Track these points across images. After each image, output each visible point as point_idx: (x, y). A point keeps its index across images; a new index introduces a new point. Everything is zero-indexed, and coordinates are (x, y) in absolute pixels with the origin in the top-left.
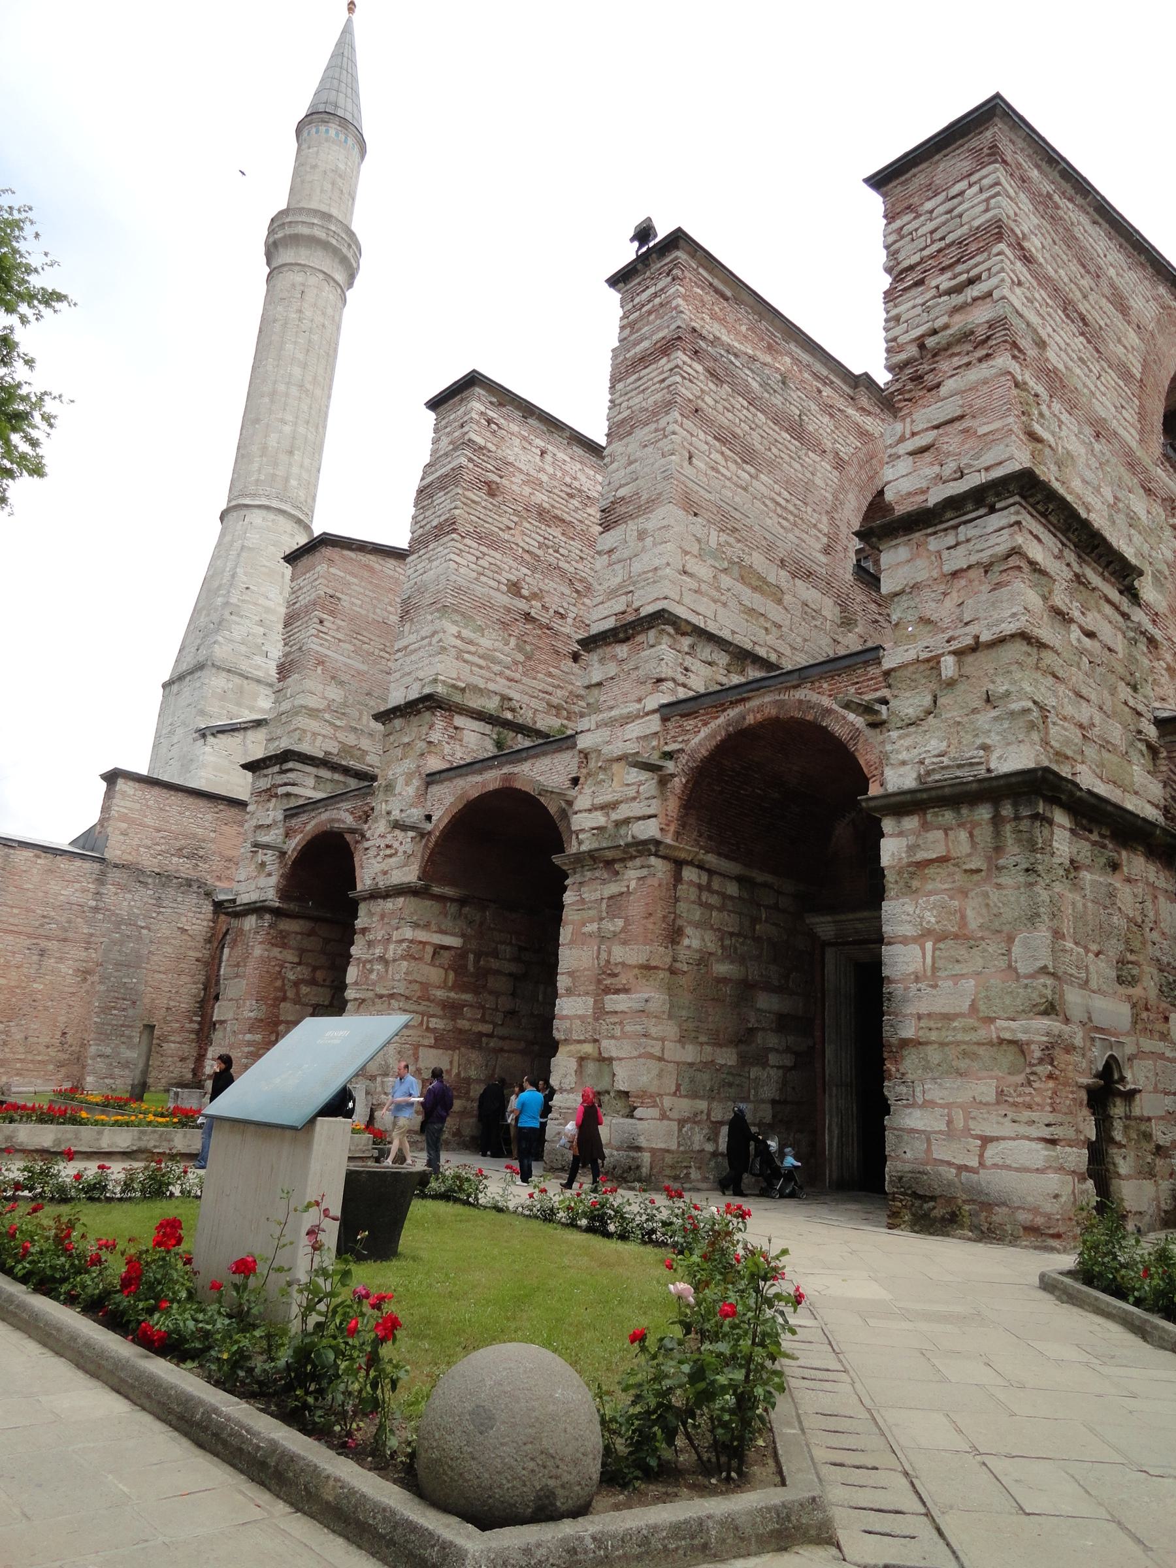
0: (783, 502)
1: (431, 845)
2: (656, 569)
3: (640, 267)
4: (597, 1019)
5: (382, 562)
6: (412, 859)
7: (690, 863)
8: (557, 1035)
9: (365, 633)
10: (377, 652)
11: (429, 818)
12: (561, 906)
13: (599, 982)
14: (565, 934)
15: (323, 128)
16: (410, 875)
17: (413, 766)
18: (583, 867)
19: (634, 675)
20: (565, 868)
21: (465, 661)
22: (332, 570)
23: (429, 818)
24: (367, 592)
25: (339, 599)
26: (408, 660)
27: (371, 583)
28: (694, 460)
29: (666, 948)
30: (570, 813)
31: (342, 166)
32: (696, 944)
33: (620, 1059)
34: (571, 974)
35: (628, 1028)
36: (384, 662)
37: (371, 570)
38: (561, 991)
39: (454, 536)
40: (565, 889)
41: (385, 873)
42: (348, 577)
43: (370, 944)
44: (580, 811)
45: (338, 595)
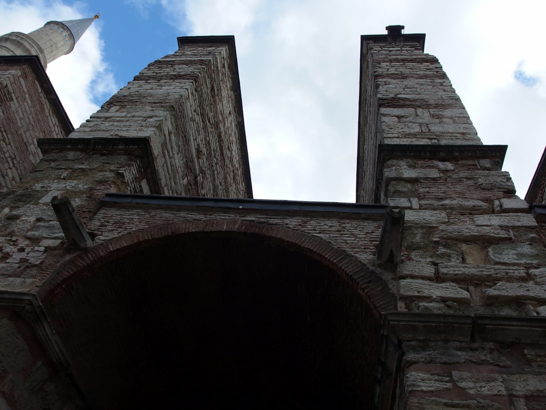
1: (82, 263)
2: (463, 134)
3: (390, 39)
5: (51, 113)
6: (34, 271)
9: (9, 136)
10: (7, 155)
15: (61, 30)
18: (446, 341)
19: (471, 182)
21: (163, 153)
22: (22, 80)
24: (30, 117)
25: (12, 99)
26: (107, 124)
27: (37, 114)
30: (387, 276)
31: (59, 45)
36: (6, 165)
37: (43, 110)
39: (192, 81)
42: (27, 95)
44: (413, 277)
45: (13, 94)
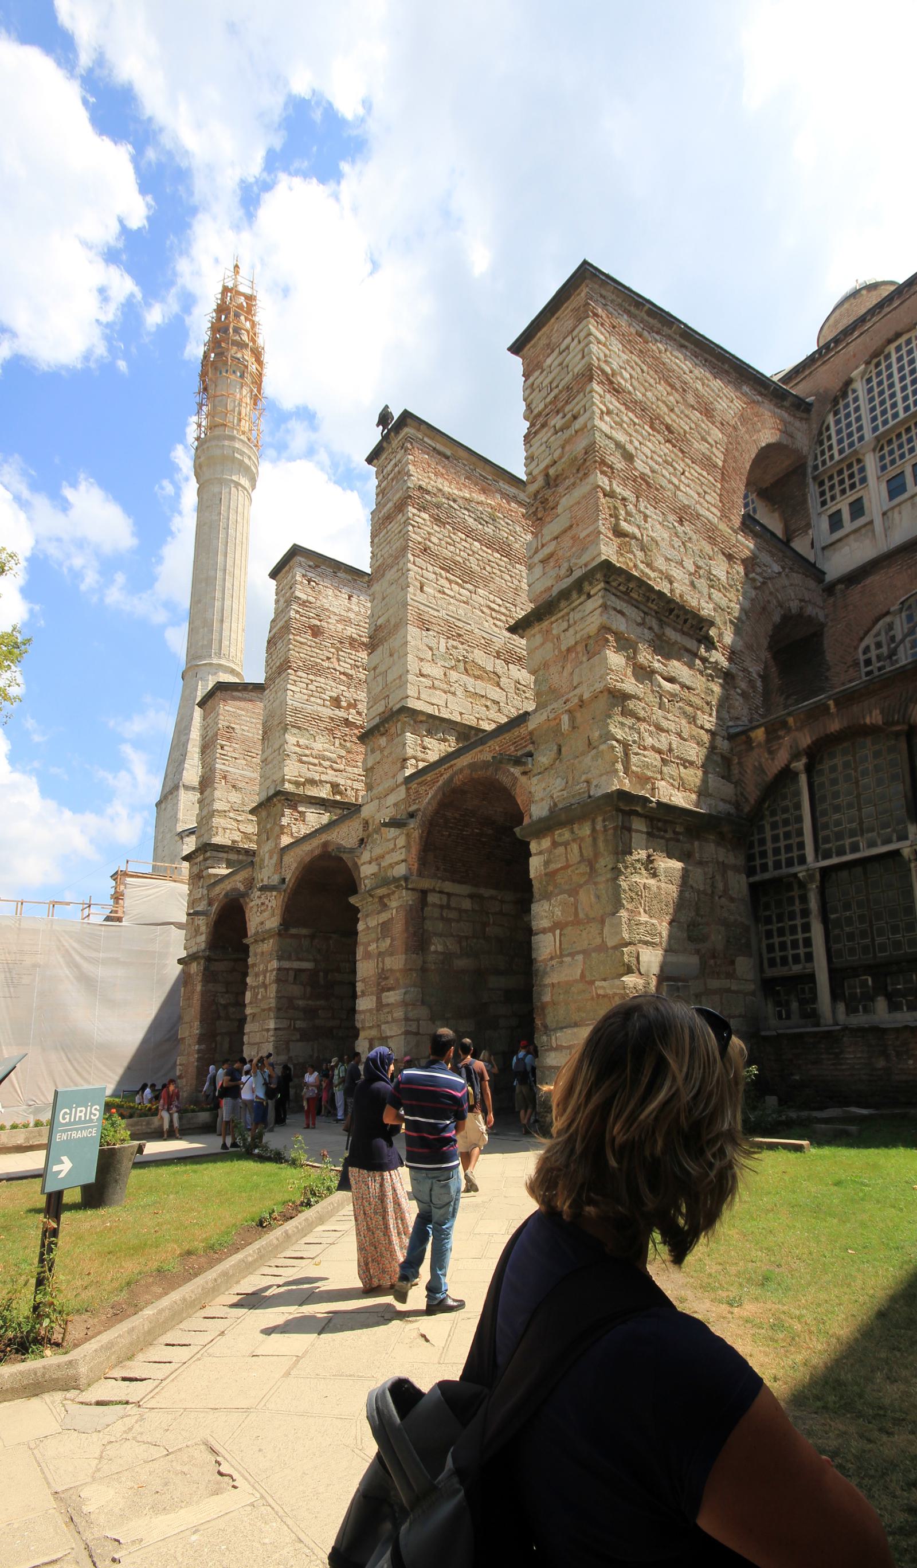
0: (496, 607)
4: (378, 1010)
7: (434, 890)
8: (359, 1025)
11: (283, 880)
12: (356, 933)
13: (379, 984)
14: (360, 954)
16: (273, 923)
17: (273, 845)
20: (357, 905)
23: (283, 880)
28: (425, 588)
29: (417, 954)
32: (440, 948)
33: (392, 1037)
34: (363, 981)
35: (395, 1015)
38: (359, 993)
40: (358, 920)
41: (262, 923)
43: (257, 975)
